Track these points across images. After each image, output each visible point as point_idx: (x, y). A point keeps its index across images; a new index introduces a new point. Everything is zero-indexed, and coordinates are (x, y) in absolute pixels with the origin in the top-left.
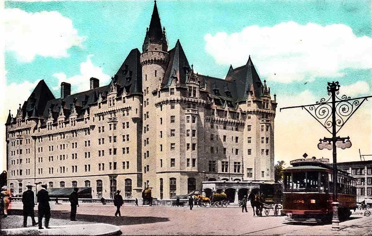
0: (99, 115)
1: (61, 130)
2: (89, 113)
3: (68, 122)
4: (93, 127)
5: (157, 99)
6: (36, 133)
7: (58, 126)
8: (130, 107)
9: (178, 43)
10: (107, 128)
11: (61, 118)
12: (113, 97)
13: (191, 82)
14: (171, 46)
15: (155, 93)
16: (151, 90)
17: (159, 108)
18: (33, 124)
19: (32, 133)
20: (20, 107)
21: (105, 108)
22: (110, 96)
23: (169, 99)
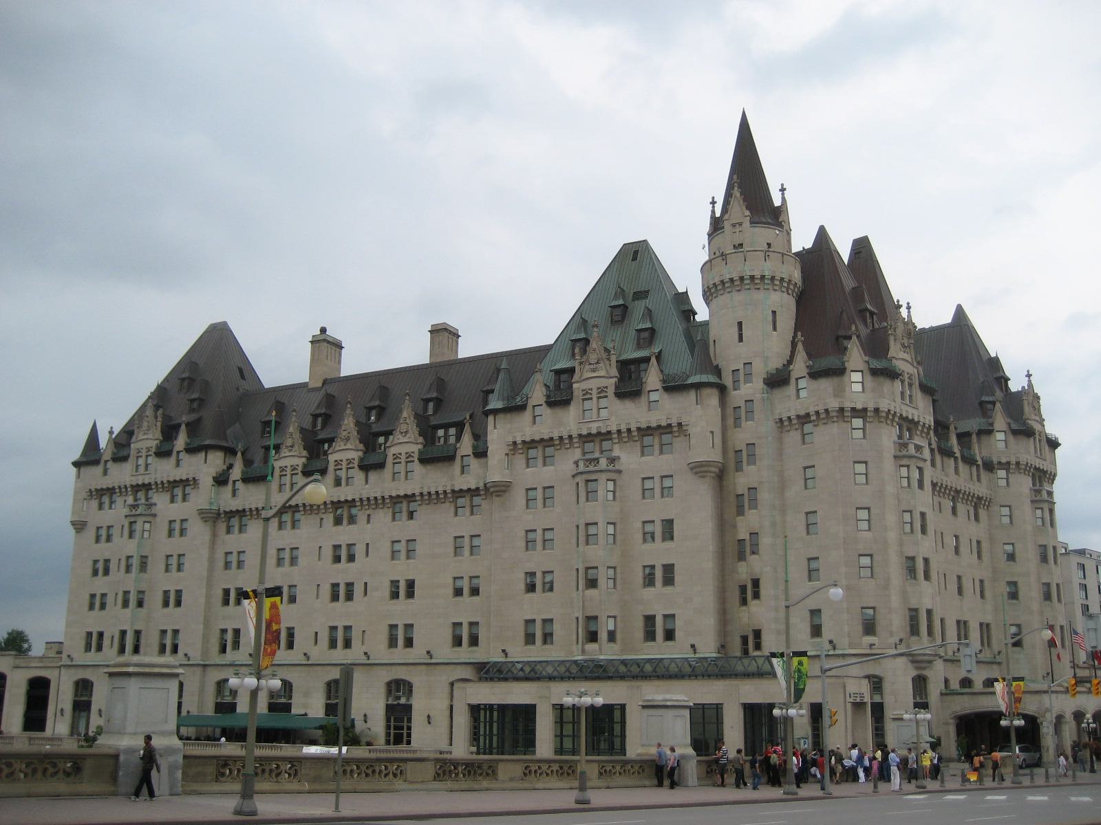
0: (530, 444)
1: (345, 493)
2: (479, 437)
3: (381, 466)
5: (791, 402)
6: (227, 501)
8: (680, 425)
10: (564, 494)
11: (346, 451)
12: (598, 388)
14: (802, 239)
15: (778, 380)
16: (760, 370)
17: (795, 432)
18: (205, 467)
19: (204, 496)
21: (570, 421)
22: (584, 385)
23: (848, 405)
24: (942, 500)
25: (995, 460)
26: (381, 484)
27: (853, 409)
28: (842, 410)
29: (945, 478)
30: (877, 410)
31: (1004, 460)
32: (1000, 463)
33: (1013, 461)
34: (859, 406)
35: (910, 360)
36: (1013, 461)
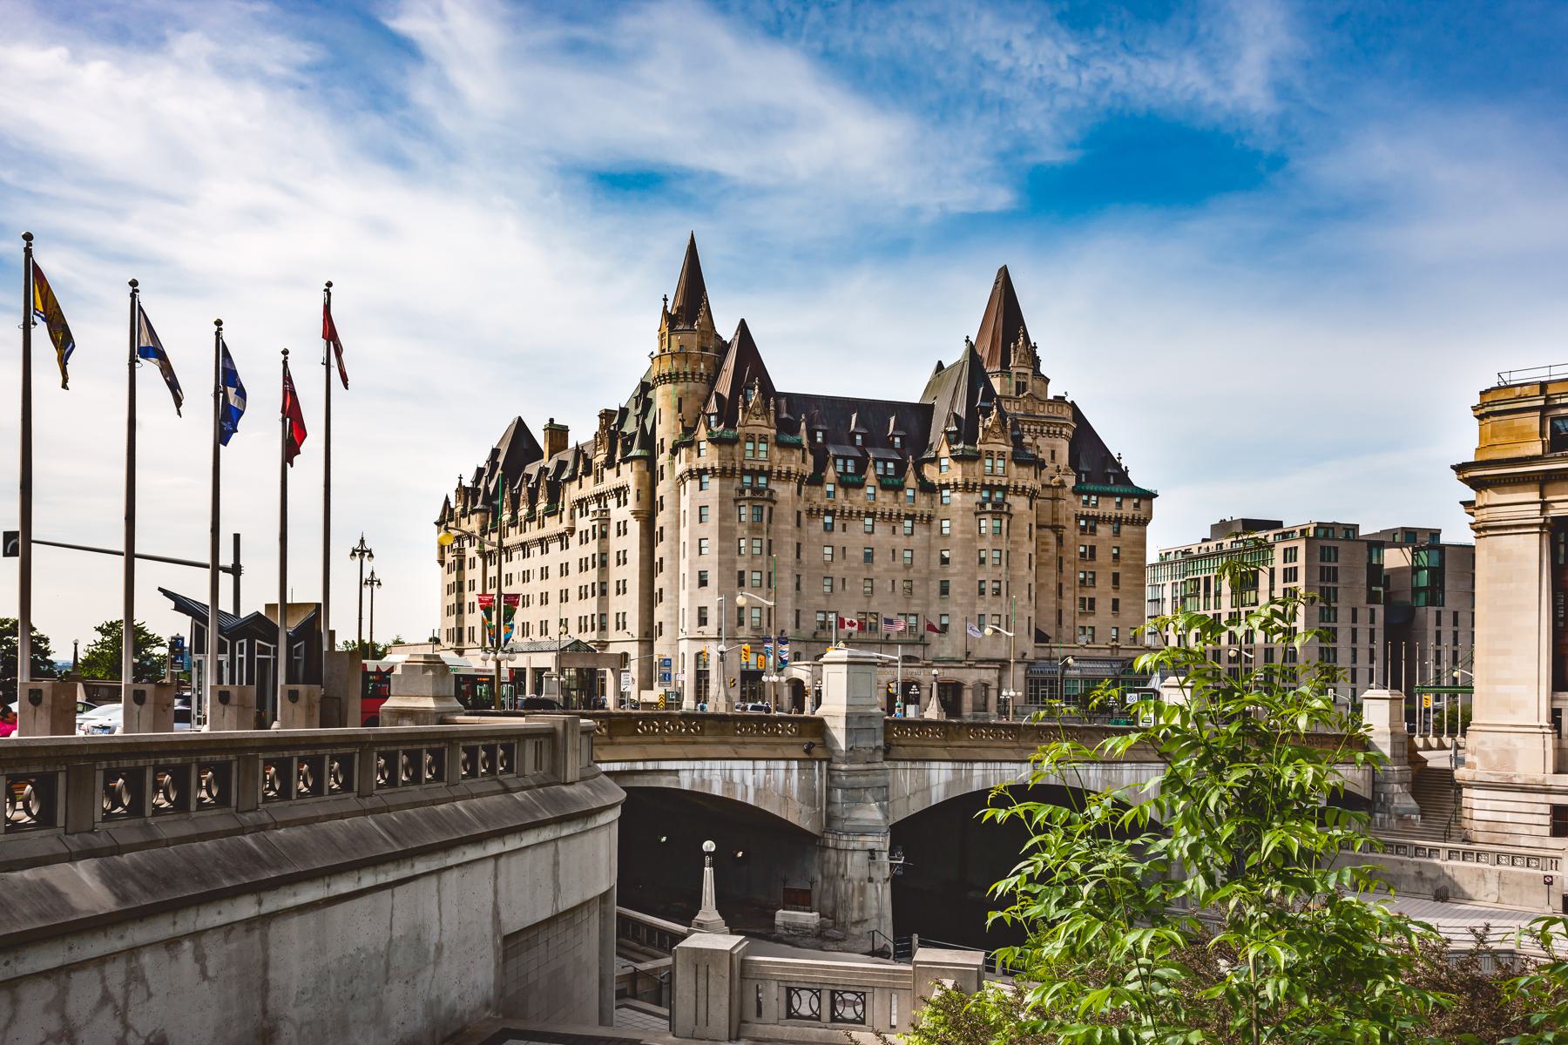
0: (581, 502)
4: (572, 531)
7: (518, 528)
9: (743, 324)
13: (750, 422)
16: (668, 445)
20: (460, 484)
23: (694, 467)
24: (851, 525)
25: (936, 482)
26: (533, 532)
27: (698, 470)
28: (690, 471)
29: (847, 505)
30: (713, 469)
31: (943, 482)
32: (940, 485)
33: (952, 481)
34: (701, 467)
35: (766, 424)
36: (952, 481)
